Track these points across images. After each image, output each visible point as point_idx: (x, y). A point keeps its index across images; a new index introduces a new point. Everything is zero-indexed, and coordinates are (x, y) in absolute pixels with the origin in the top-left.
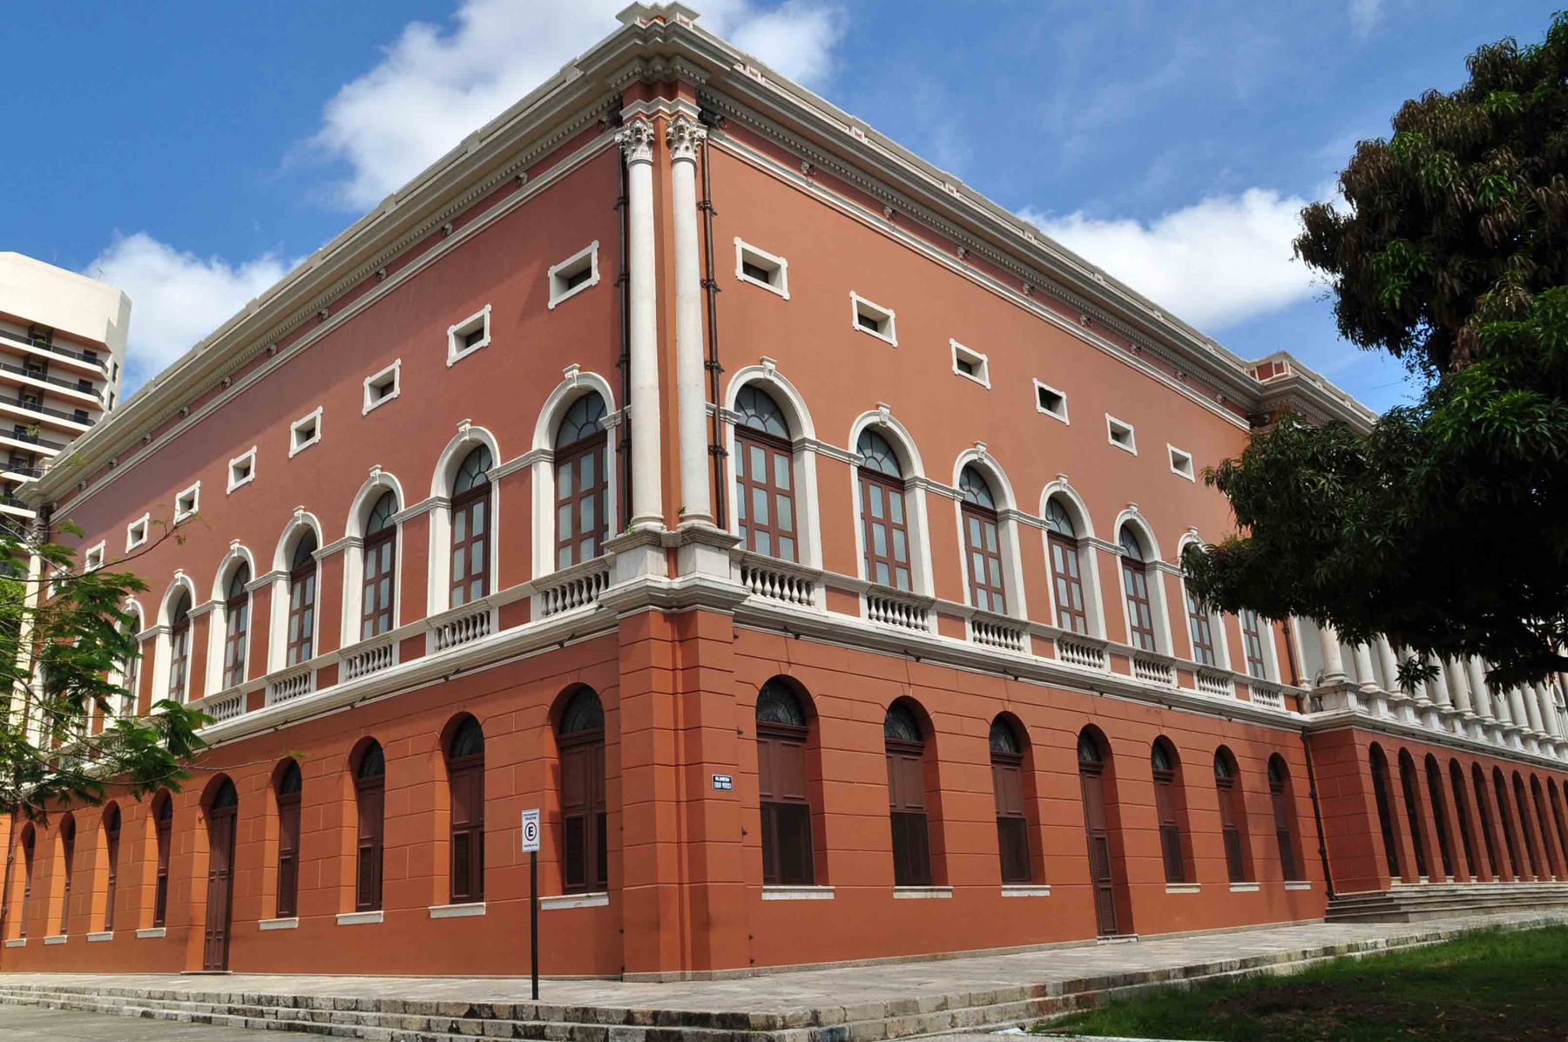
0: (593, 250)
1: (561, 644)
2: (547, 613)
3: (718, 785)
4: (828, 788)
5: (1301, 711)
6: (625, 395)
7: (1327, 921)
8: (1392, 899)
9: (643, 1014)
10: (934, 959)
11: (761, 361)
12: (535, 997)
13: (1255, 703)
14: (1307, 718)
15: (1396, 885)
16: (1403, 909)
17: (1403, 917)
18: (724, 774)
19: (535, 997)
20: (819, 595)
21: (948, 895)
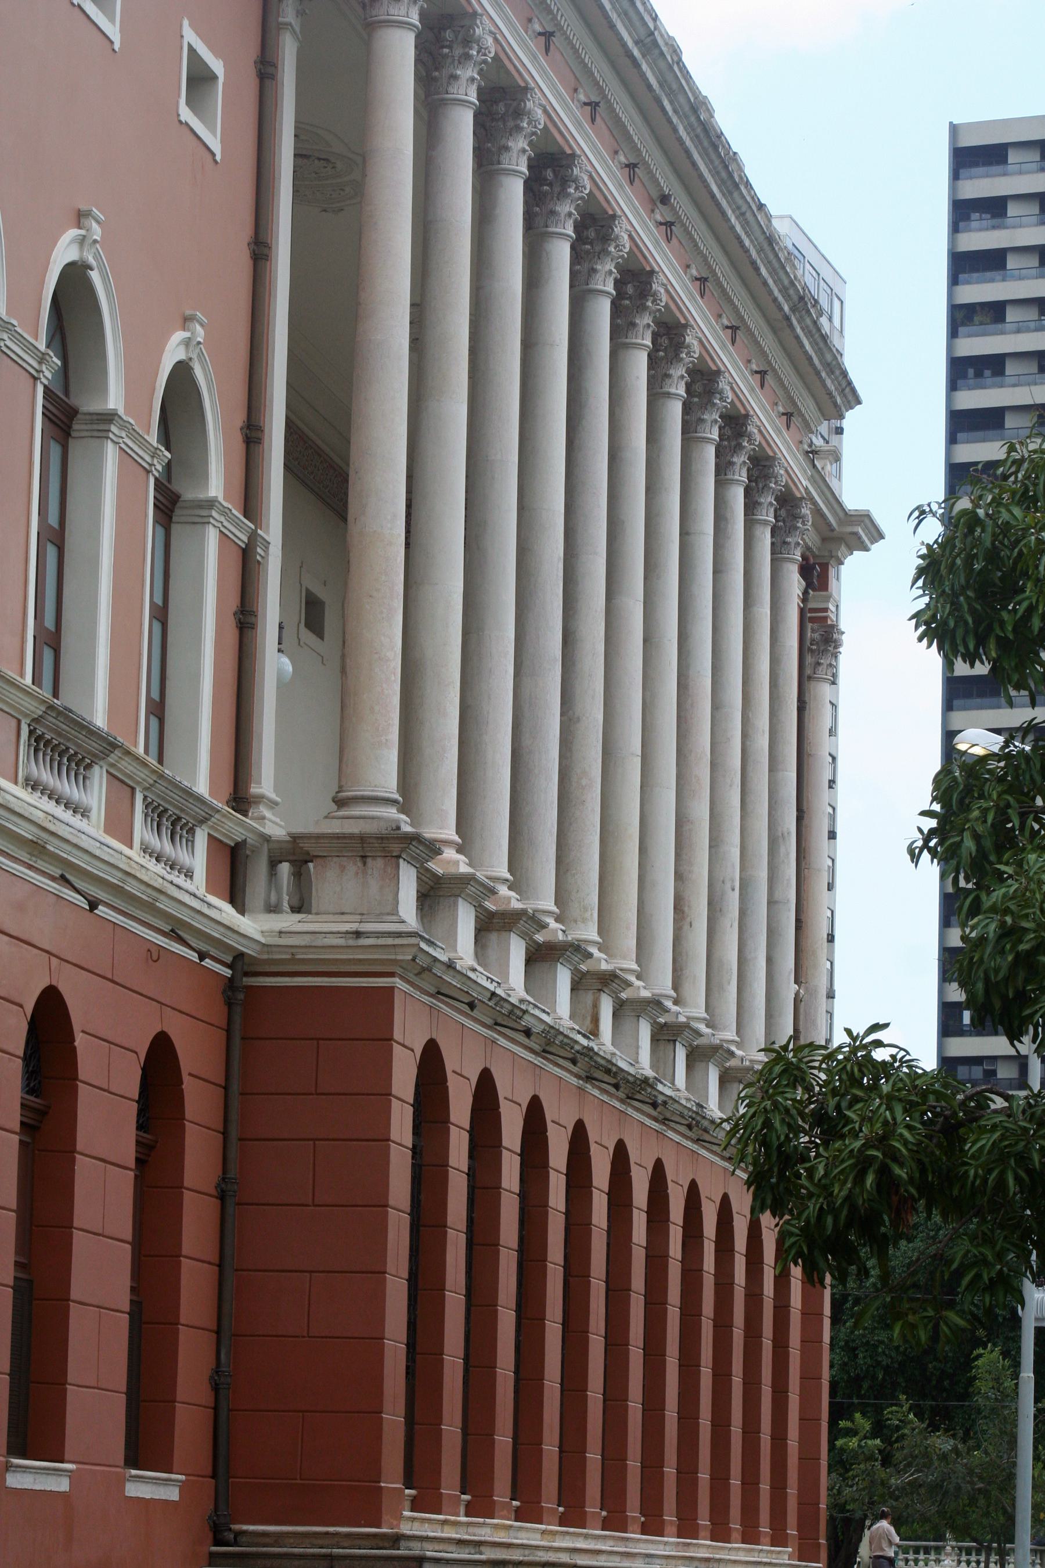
5: (236, 897)
13: (137, 854)
14: (254, 927)
15: (414, 1524)
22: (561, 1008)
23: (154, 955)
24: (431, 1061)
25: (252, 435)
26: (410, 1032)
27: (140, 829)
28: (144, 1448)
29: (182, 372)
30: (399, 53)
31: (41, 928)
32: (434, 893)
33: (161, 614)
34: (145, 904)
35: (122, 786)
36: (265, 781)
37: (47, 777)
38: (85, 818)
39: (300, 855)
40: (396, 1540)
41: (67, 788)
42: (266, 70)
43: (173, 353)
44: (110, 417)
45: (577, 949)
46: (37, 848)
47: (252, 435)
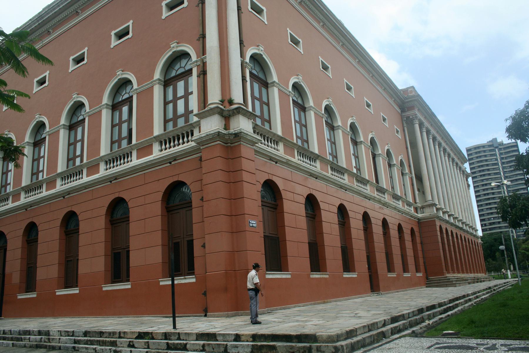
2: (161, 150)
3: (251, 225)
4: (287, 229)
5: (417, 213)
7: (427, 287)
8: (449, 279)
9: (246, 335)
10: (324, 303)
11: (258, 46)
12: (175, 327)
13: (406, 208)
14: (420, 215)
15: (448, 275)
16: (454, 282)
17: (454, 285)
18: (253, 220)
19: (175, 327)
20: (281, 147)
21: (327, 276)
22: (452, 221)
23: (410, 219)
24: (440, 227)
25: (410, 166)
26: (438, 223)
27: (406, 206)
28: (418, 271)
29: (401, 160)
30: (417, 127)
31: (397, 217)
32: (438, 210)
33: (404, 185)
34: (408, 214)
35: (403, 202)
36: (418, 201)
37: (395, 201)
38: (400, 204)
39: (423, 208)
41: (397, 202)
43: (400, 158)
44: (395, 164)
45: (453, 215)
46: (395, 208)
47: (410, 166)
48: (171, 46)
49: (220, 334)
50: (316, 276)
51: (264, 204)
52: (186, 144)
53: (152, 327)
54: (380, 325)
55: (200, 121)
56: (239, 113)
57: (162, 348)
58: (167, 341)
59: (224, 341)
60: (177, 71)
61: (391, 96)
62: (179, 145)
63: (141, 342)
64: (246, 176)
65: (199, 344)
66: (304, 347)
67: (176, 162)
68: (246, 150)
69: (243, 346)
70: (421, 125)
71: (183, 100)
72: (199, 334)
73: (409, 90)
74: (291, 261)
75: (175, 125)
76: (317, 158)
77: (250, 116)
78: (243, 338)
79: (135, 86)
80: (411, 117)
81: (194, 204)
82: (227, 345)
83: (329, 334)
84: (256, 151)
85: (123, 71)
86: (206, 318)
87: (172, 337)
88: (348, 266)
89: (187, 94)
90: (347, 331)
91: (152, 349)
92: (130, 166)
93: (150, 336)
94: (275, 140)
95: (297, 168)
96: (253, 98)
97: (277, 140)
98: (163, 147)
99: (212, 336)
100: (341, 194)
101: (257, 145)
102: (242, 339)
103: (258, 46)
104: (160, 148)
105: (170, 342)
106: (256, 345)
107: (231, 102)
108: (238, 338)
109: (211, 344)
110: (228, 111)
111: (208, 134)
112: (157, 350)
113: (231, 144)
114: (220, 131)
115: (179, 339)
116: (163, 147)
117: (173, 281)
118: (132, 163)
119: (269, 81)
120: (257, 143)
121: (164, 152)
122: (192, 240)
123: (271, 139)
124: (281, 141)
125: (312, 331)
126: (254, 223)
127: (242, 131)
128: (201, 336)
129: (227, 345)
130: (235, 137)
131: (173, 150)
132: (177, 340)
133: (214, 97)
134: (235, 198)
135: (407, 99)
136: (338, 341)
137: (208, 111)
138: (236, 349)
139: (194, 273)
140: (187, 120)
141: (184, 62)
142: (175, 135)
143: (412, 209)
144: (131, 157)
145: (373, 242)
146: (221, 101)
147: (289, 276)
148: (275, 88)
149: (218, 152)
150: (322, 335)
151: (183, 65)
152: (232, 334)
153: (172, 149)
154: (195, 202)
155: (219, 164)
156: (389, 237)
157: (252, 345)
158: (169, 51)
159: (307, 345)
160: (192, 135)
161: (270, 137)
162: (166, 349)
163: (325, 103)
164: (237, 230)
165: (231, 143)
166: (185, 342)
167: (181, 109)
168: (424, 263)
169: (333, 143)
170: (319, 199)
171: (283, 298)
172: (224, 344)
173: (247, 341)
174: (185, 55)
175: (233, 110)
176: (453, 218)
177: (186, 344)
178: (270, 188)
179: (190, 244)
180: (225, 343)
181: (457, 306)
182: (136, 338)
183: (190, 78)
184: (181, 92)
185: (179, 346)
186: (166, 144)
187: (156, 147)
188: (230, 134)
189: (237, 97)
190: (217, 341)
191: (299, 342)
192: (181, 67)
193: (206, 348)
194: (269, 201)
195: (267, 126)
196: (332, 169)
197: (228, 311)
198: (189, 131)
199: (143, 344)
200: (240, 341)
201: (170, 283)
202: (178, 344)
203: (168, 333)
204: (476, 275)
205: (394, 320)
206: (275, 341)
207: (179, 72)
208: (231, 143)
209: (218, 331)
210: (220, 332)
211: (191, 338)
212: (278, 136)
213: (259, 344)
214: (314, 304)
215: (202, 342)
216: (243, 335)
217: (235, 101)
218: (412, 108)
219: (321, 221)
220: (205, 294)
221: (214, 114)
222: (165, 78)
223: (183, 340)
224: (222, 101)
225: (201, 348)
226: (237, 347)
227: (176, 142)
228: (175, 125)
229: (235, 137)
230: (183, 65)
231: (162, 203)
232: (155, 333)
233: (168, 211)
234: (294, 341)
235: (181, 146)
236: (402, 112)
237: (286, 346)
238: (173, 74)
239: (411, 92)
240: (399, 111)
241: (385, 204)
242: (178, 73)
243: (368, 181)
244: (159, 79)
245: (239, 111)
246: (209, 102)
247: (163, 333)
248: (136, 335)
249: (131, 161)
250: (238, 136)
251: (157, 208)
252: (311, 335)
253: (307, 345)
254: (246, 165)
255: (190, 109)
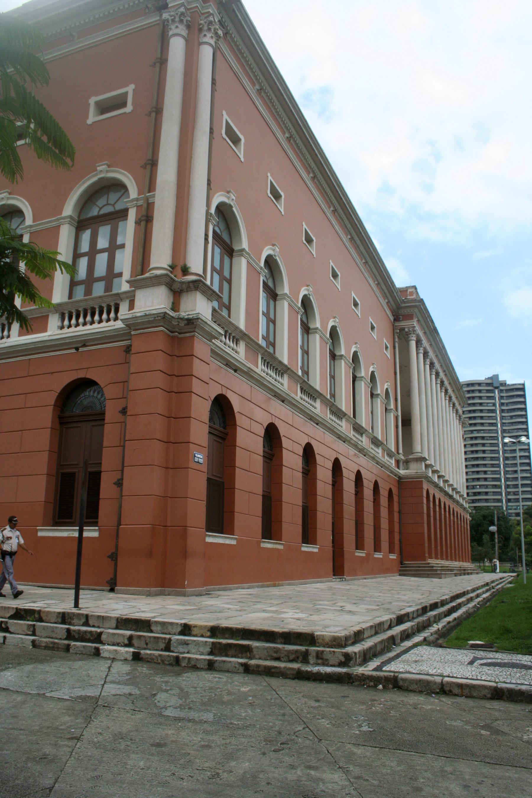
0: (130, 89)
1: (77, 349)
2: (62, 328)
5: (398, 467)
6: (149, 184)
7: (400, 575)
8: (433, 567)
9: (201, 627)
10: (275, 586)
11: (228, 192)
12: (76, 605)
14: (402, 472)
16: (439, 572)
18: (200, 452)
19: (76, 605)
23: (389, 476)
25: (396, 400)
26: (425, 486)
27: (386, 457)
28: (391, 551)
29: (387, 389)
30: (413, 344)
32: (427, 466)
34: (387, 468)
35: (383, 450)
36: (401, 451)
37: (373, 447)
40: (429, 563)
42: (394, 348)
43: (386, 387)
44: (378, 395)
45: (444, 476)
47: (396, 400)
48: (98, 168)
49: (157, 623)
50: (268, 545)
51: (213, 431)
52: (104, 324)
53: (34, 602)
54: (386, 626)
55: (134, 291)
56: (196, 288)
57: (59, 637)
58: (67, 626)
59: (163, 633)
60: (101, 209)
61: (385, 296)
62: (92, 323)
63: (21, 624)
64: (196, 386)
65: (123, 636)
66: (297, 651)
67: (85, 349)
68: (201, 348)
69: (197, 643)
70: (419, 342)
71: (105, 255)
72: (122, 619)
73: (409, 290)
74: (238, 519)
75: (88, 291)
76: (285, 372)
77: (210, 294)
78: (195, 631)
79: (29, 221)
80: (406, 330)
81: (108, 417)
82: (170, 640)
83: (335, 634)
84: (212, 351)
85: (10, 194)
86: (112, 595)
87: (75, 621)
88: (308, 536)
89: (114, 248)
90: (355, 632)
91: (41, 637)
92: (6, 345)
93: (37, 616)
94: (236, 335)
95: (259, 382)
96: (213, 269)
97: (237, 337)
98: (66, 322)
99: (144, 625)
100: (310, 428)
101: (213, 341)
102: (194, 633)
103: (228, 192)
104: (60, 324)
105: (72, 628)
106: (220, 643)
107: (185, 271)
108: (186, 630)
109: (144, 636)
110: (179, 283)
111: (147, 313)
112: (51, 640)
113: (180, 333)
114: (168, 312)
115: (86, 624)
116: (66, 322)
117: (81, 532)
118: (9, 340)
119: (236, 248)
120: (216, 338)
121: (66, 330)
122: (99, 473)
123: (230, 334)
124: (243, 339)
125: (302, 628)
126: (200, 457)
127: (200, 316)
128: (123, 623)
129: (170, 640)
130: (188, 324)
131: (82, 330)
132: (83, 625)
133: (161, 258)
134: (177, 417)
135: (405, 303)
136: (345, 646)
137: (150, 278)
138: (185, 646)
139: (97, 522)
140: (108, 288)
141: (113, 197)
142: (88, 307)
143: (393, 462)
144: (9, 330)
145: (342, 503)
146: (170, 266)
147: (234, 542)
148: (243, 259)
149: (160, 343)
150: (323, 636)
151: (112, 201)
152: (177, 624)
153: (80, 328)
154: (111, 413)
155: (160, 361)
156: (362, 498)
157: (213, 643)
158: (94, 176)
159: (303, 648)
160: (117, 311)
161: (230, 332)
162: (66, 639)
163: (303, 292)
164: (175, 465)
165: (179, 333)
166: (99, 630)
167: (101, 269)
168: (400, 541)
169: (306, 352)
170: (282, 432)
171: (223, 574)
172: (165, 638)
173: (202, 636)
174: (118, 187)
175: (189, 282)
176: (443, 481)
177: (101, 634)
178: (222, 407)
179: (95, 479)
180: (168, 636)
181: (459, 606)
182: (11, 617)
183: (121, 224)
184: (103, 243)
185: (89, 636)
186: (70, 319)
187: (54, 321)
188: (181, 319)
189: (195, 264)
190: (151, 631)
191: (285, 643)
192: (108, 204)
193: (135, 642)
194: (217, 426)
195: (225, 313)
196: (302, 389)
197: (150, 586)
198: (112, 304)
199: (26, 627)
200: (190, 635)
201: (76, 534)
202: (86, 632)
203: (68, 613)
204: (461, 563)
205: (400, 620)
206: (247, 639)
207: (104, 211)
208: (179, 333)
209: (154, 617)
210: (156, 619)
211: (107, 624)
212: (241, 331)
213: (224, 641)
214: (262, 586)
215: (128, 633)
216: (195, 626)
217: (193, 270)
218: (409, 317)
219: (281, 465)
220: (114, 557)
221: (159, 284)
222: (79, 216)
223: (94, 626)
224: (173, 267)
225: (126, 642)
226: (188, 644)
227: (89, 318)
228: (88, 291)
229: (188, 324)
230: (111, 201)
231: (54, 409)
232: (44, 612)
233: (62, 423)
234: (279, 641)
235: (96, 325)
236: (395, 320)
237: (267, 648)
238: (94, 212)
239: (411, 294)
240: (392, 318)
241: (362, 451)
242: (102, 212)
243: (345, 415)
244: (71, 217)
245: (197, 285)
246: (152, 266)
247: (59, 613)
248: (12, 612)
249: (9, 337)
250: (192, 323)
251: (46, 416)
252: (306, 633)
253: (303, 648)
254: (199, 368)
255: (117, 270)
